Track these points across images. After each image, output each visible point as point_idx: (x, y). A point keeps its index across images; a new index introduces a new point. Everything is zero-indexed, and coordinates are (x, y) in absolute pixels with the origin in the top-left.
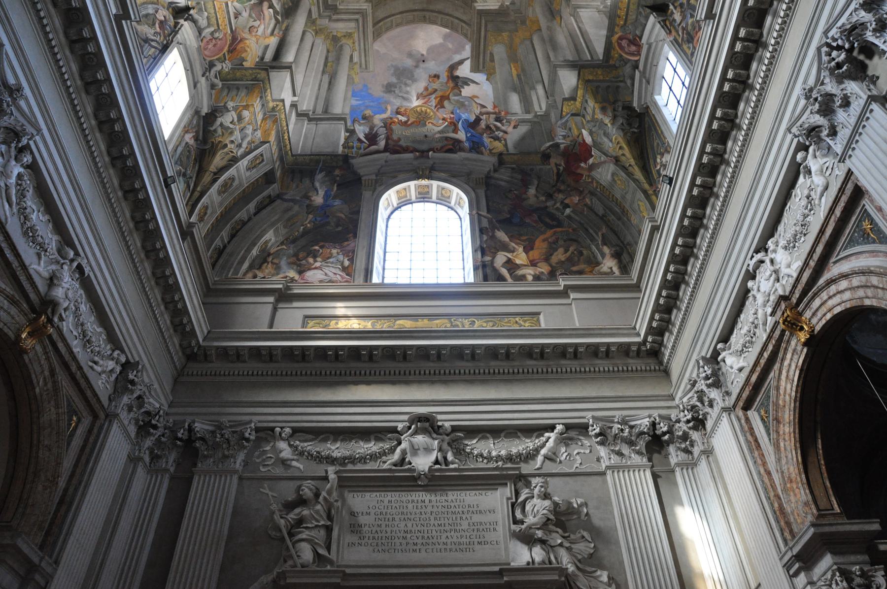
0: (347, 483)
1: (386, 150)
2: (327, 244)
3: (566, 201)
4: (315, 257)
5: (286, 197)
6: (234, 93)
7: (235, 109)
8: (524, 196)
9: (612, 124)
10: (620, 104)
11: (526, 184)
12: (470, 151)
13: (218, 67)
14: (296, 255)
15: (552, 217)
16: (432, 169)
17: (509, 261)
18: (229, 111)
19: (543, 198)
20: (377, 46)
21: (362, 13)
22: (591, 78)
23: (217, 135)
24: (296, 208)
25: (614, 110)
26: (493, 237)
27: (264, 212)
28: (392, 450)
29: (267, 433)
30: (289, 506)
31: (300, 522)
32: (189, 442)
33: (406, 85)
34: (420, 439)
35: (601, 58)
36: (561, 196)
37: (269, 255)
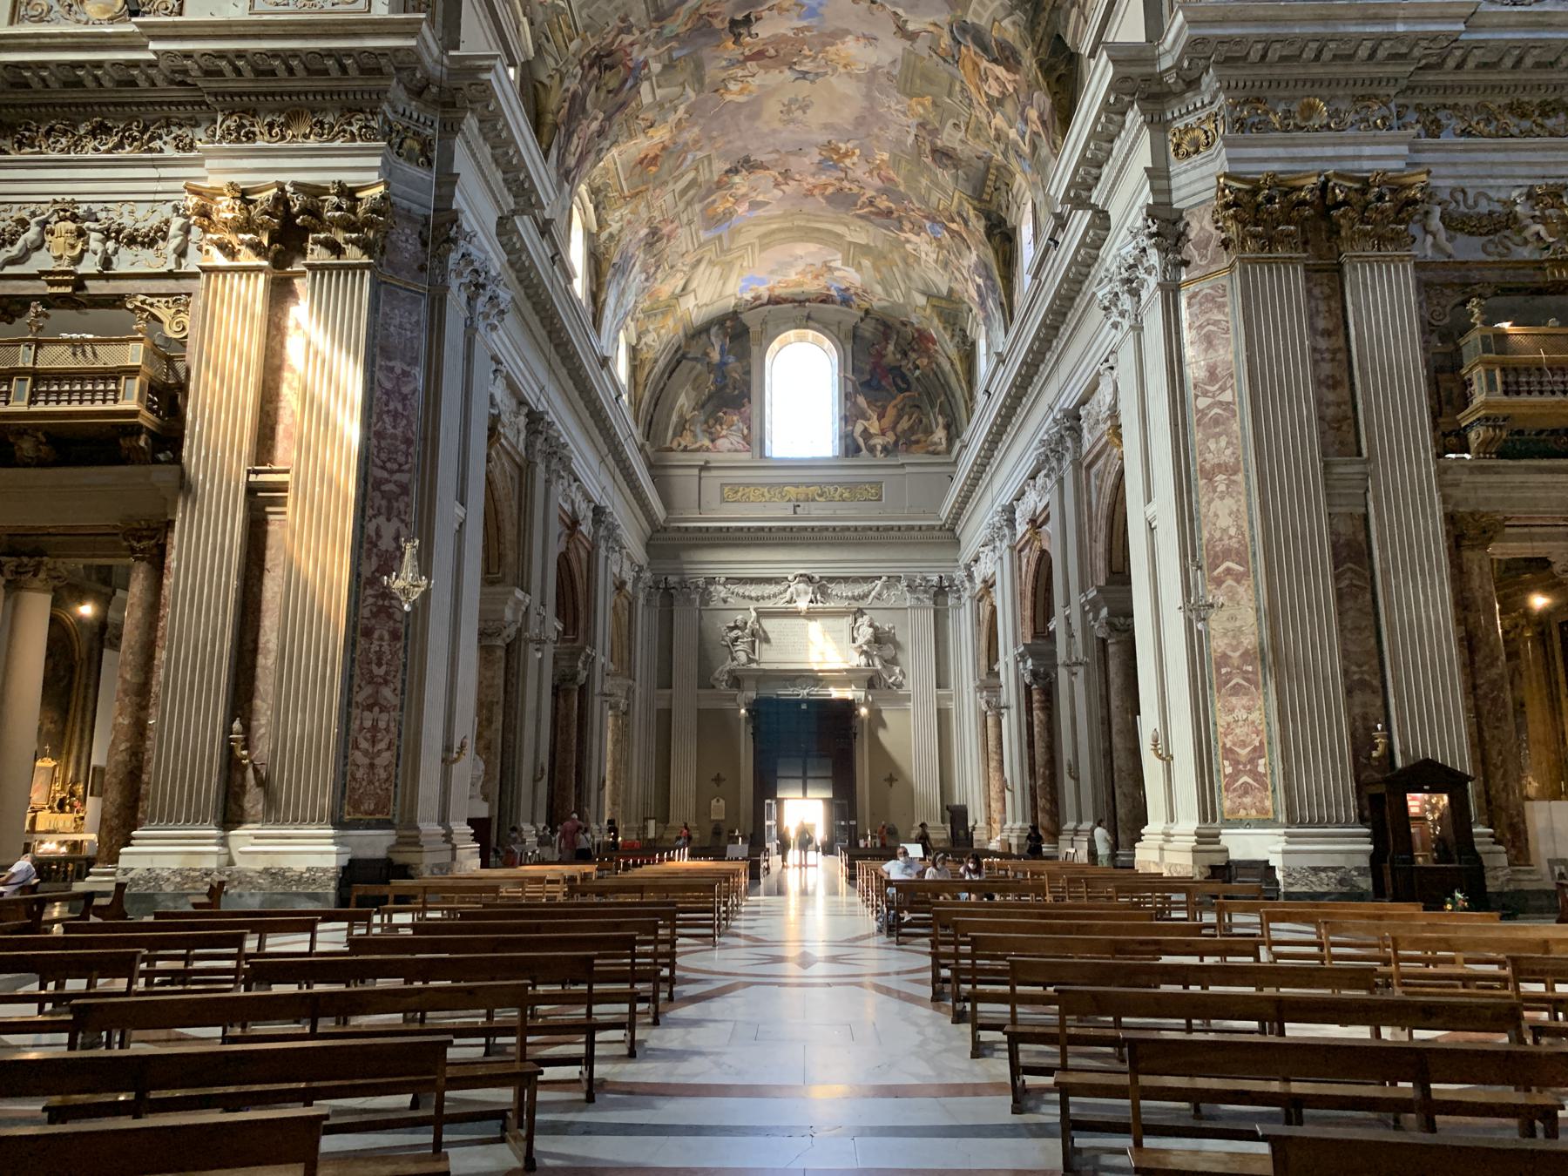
0: (762, 614)
2: (729, 410)
4: (721, 425)
5: (689, 356)
7: (655, 330)
11: (886, 338)
13: (641, 306)
14: (706, 422)
15: (904, 378)
16: (809, 318)
17: (865, 430)
19: (899, 356)
20: (764, 255)
21: (752, 245)
24: (699, 366)
26: (855, 403)
28: (785, 591)
29: (711, 581)
30: (732, 629)
31: (737, 639)
32: (667, 589)
34: (802, 586)
36: (913, 355)
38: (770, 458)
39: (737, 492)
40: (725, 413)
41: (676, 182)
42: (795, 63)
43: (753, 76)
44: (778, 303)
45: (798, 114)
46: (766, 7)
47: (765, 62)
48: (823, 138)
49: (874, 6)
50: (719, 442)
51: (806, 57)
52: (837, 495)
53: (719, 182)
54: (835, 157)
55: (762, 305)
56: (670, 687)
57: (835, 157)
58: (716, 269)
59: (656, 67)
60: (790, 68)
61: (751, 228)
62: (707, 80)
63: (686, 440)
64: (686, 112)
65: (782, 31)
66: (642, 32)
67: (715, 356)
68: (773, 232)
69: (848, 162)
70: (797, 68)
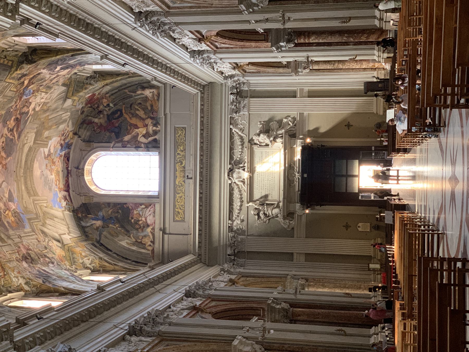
0: (251, 199)
2: (130, 216)
3: (105, 105)
4: (139, 221)
5: (98, 239)
7: (82, 259)
8: (99, 124)
9: (93, 85)
10: (85, 81)
11: (91, 123)
12: (70, 149)
13: (68, 267)
14: (137, 229)
15: (114, 113)
16: (78, 168)
17: (144, 136)
18: (83, 262)
19: (101, 116)
21: (34, 201)
22: (71, 93)
23: (95, 266)
24: (105, 233)
25: (87, 84)
26: (128, 142)
27: (109, 247)
28: (237, 185)
29: (230, 229)
30: (259, 217)
31: (265, 214)
32: (235, 255)
33: (48, 181)
34: (235, 175)
35: (66, 88)
36: (101, 107)
37: (136, 241)
38: (159, 192)
39: (179, 213)
40: (132, 218)
44: (68, 186)
50: (149, 222)
52: (182, 154)
55: (69, 195)
56: (292, 254)
58: (47, 222)
61: (24, 201)
63: (147, 241)
67: (99, 223)
68: (27, 188)
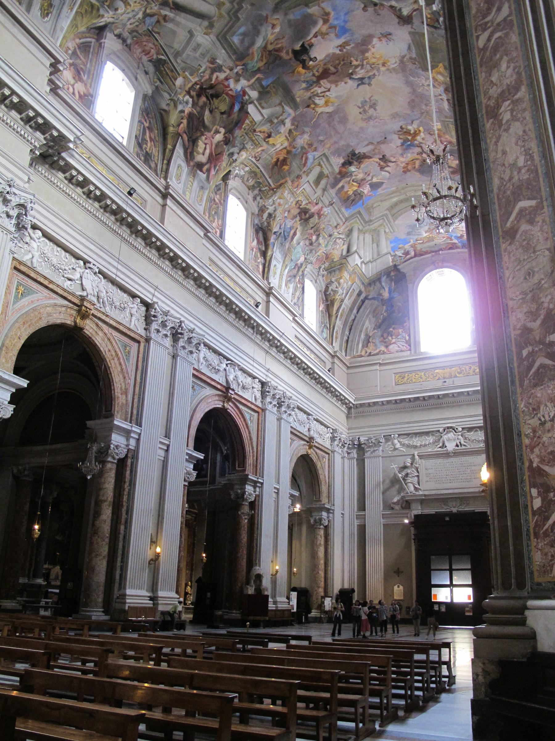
1: (415, 256)
4: (391, 336)
5: (370, 297)
6: (333, 273)
7: (336, 280)
13: (323, 267)
14: (382, 336)
20: (396, 222)
21: (386, 215)
27: (361, 310)
31: (407, 475)
32: (360, 445)
37: (370, 337)
38: (422, 353)
39: (404, 378)
40: (394, 329)
41: (307, 175)
42: (352, 74)
43: (329, 90)
45: (371, 111)
46: (311, 35)
47: (331, 78)
48: (396, 126)
49: (377, 8)
50: (391, 347)
51: (357, 67)
52: (471, 372)
53: (340, 173)
54: (410, 138)
55: (411, 258)
56: (365, 510)
57: (410, 138)
58: (367, 235)
59: (254, 94)
60: (350, 78)
61: (379, 203)
62: (298, 100)
63: (371, 348)
64: (293, 124)
65: (331, 51)
66: (231, 69)
67: (386, 295)
68: (396, 204)
69: (418, 138)
70: (354, 76)
